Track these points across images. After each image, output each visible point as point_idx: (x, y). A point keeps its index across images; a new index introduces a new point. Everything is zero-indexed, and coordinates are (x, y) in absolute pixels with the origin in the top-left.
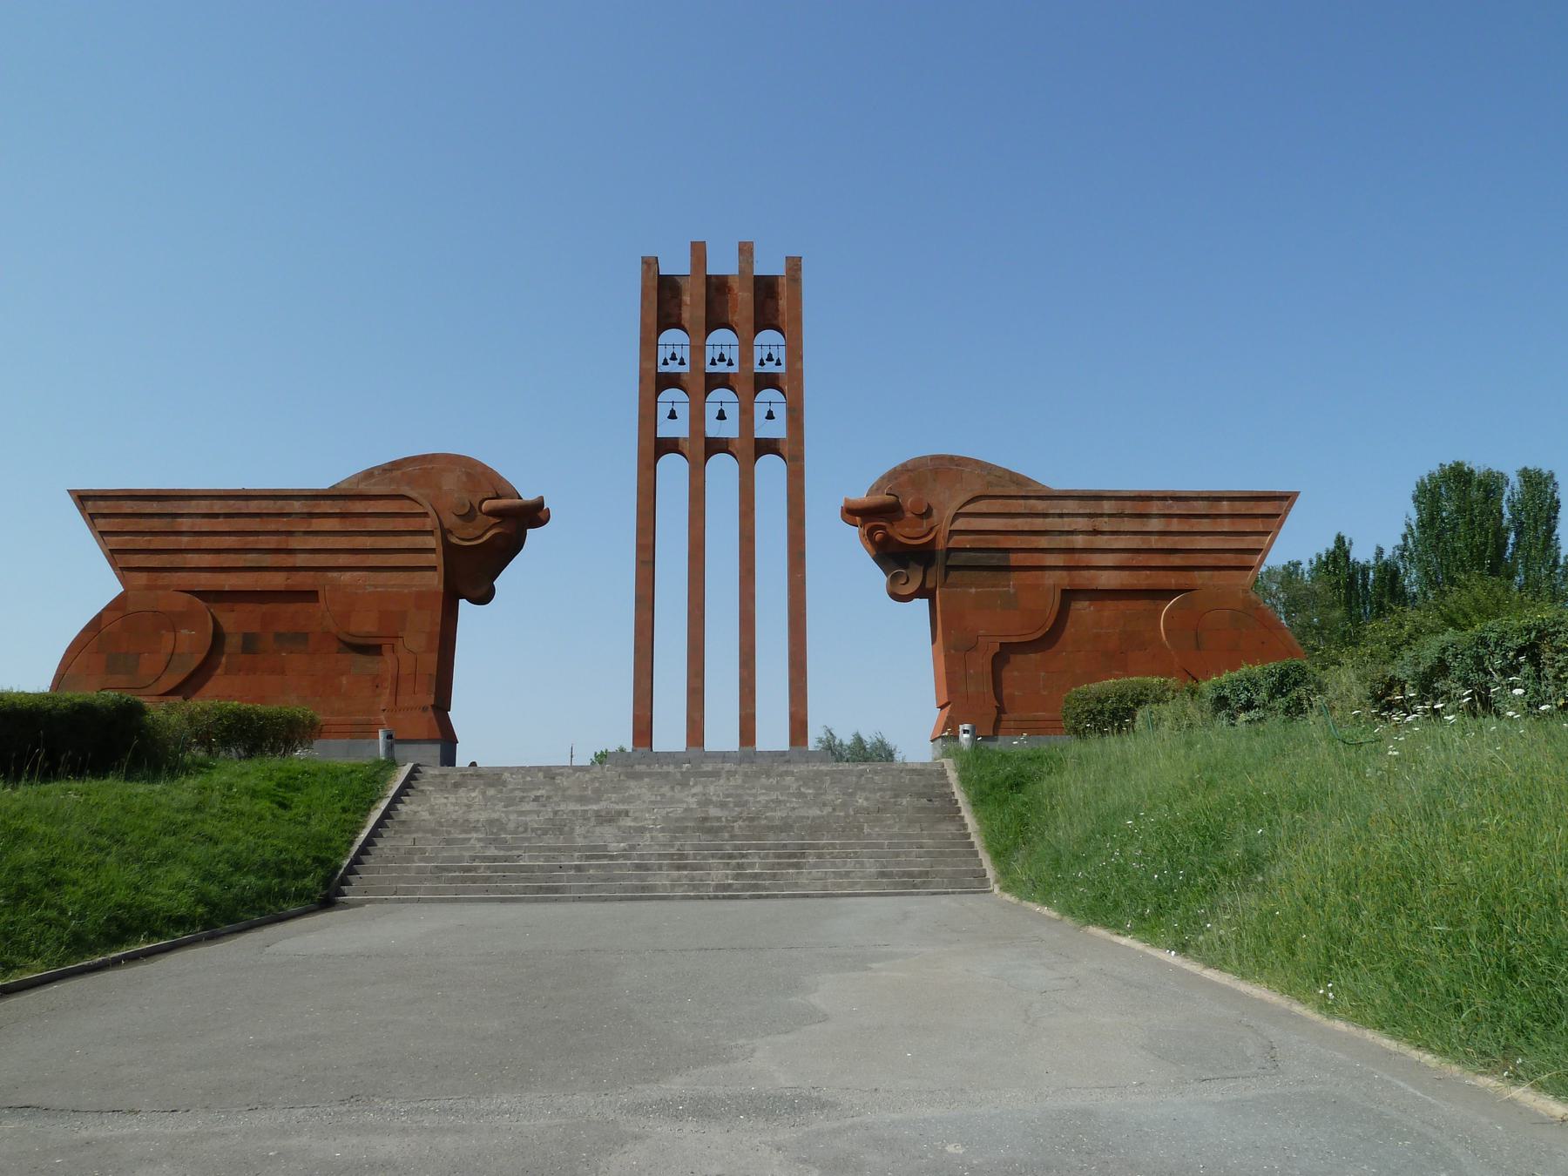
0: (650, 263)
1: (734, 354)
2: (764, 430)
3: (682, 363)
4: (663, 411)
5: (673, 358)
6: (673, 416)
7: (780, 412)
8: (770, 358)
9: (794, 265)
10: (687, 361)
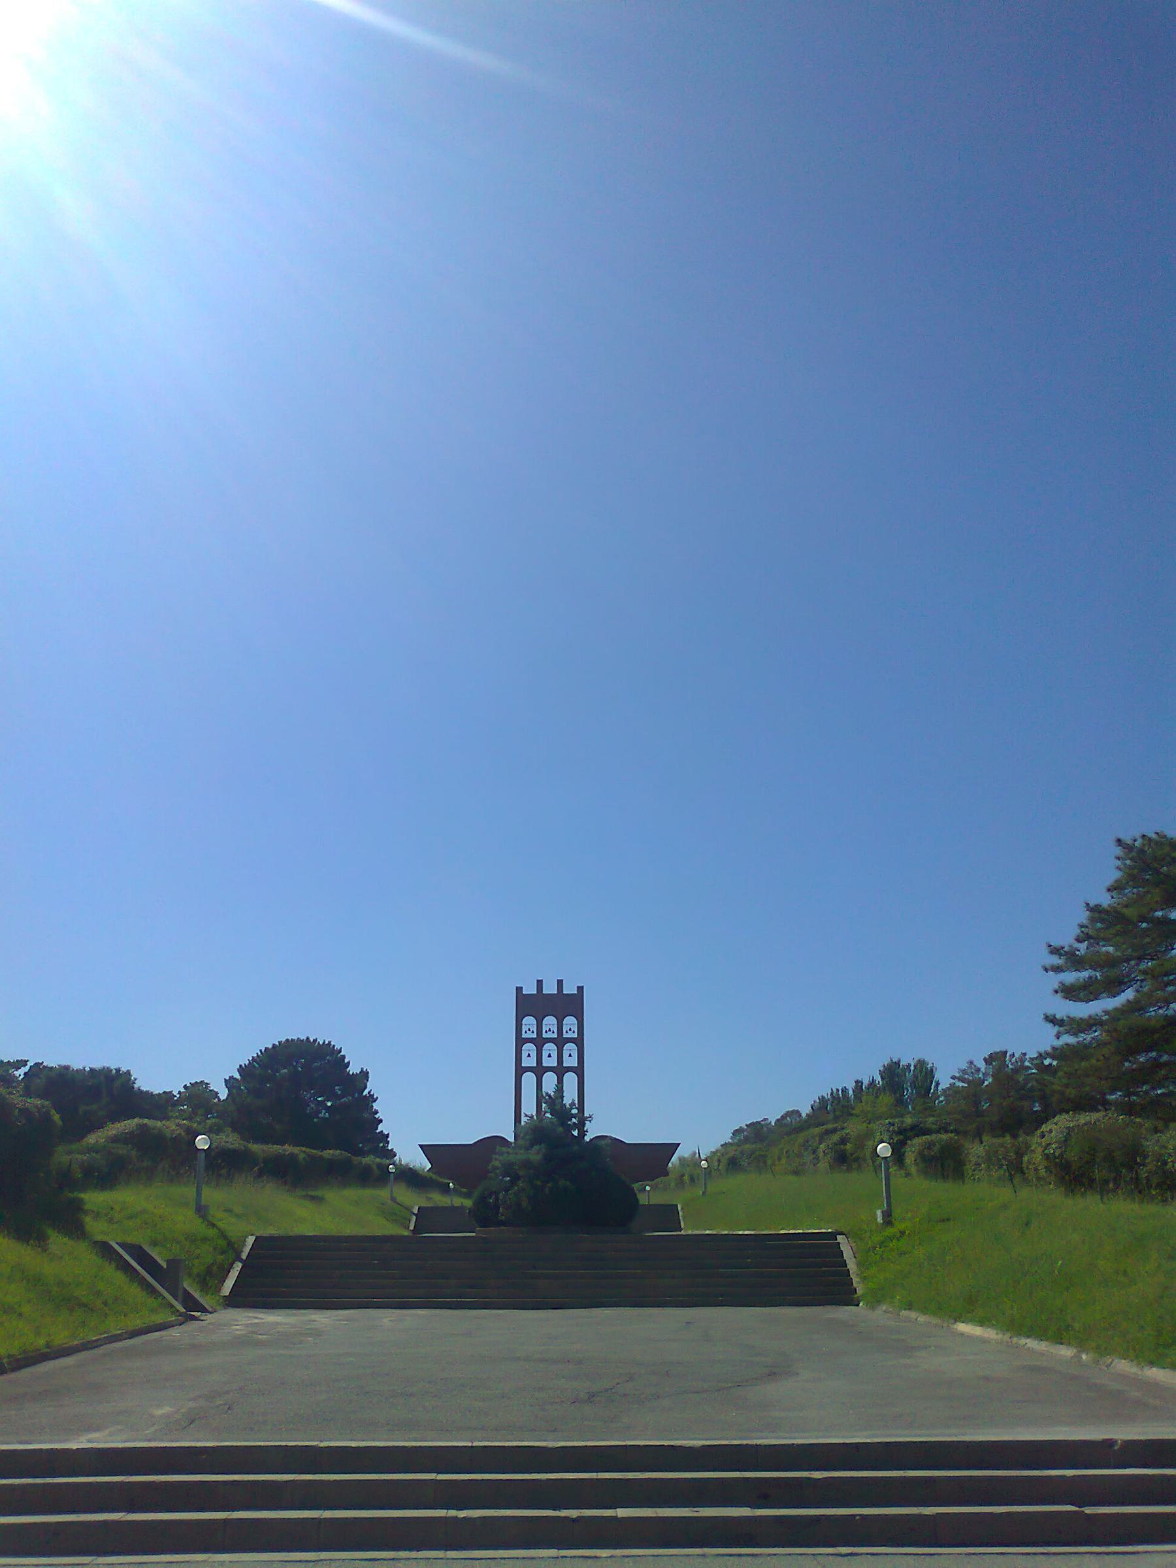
0: (519, 990)
4: (524, 1055)
9: (580, 989)
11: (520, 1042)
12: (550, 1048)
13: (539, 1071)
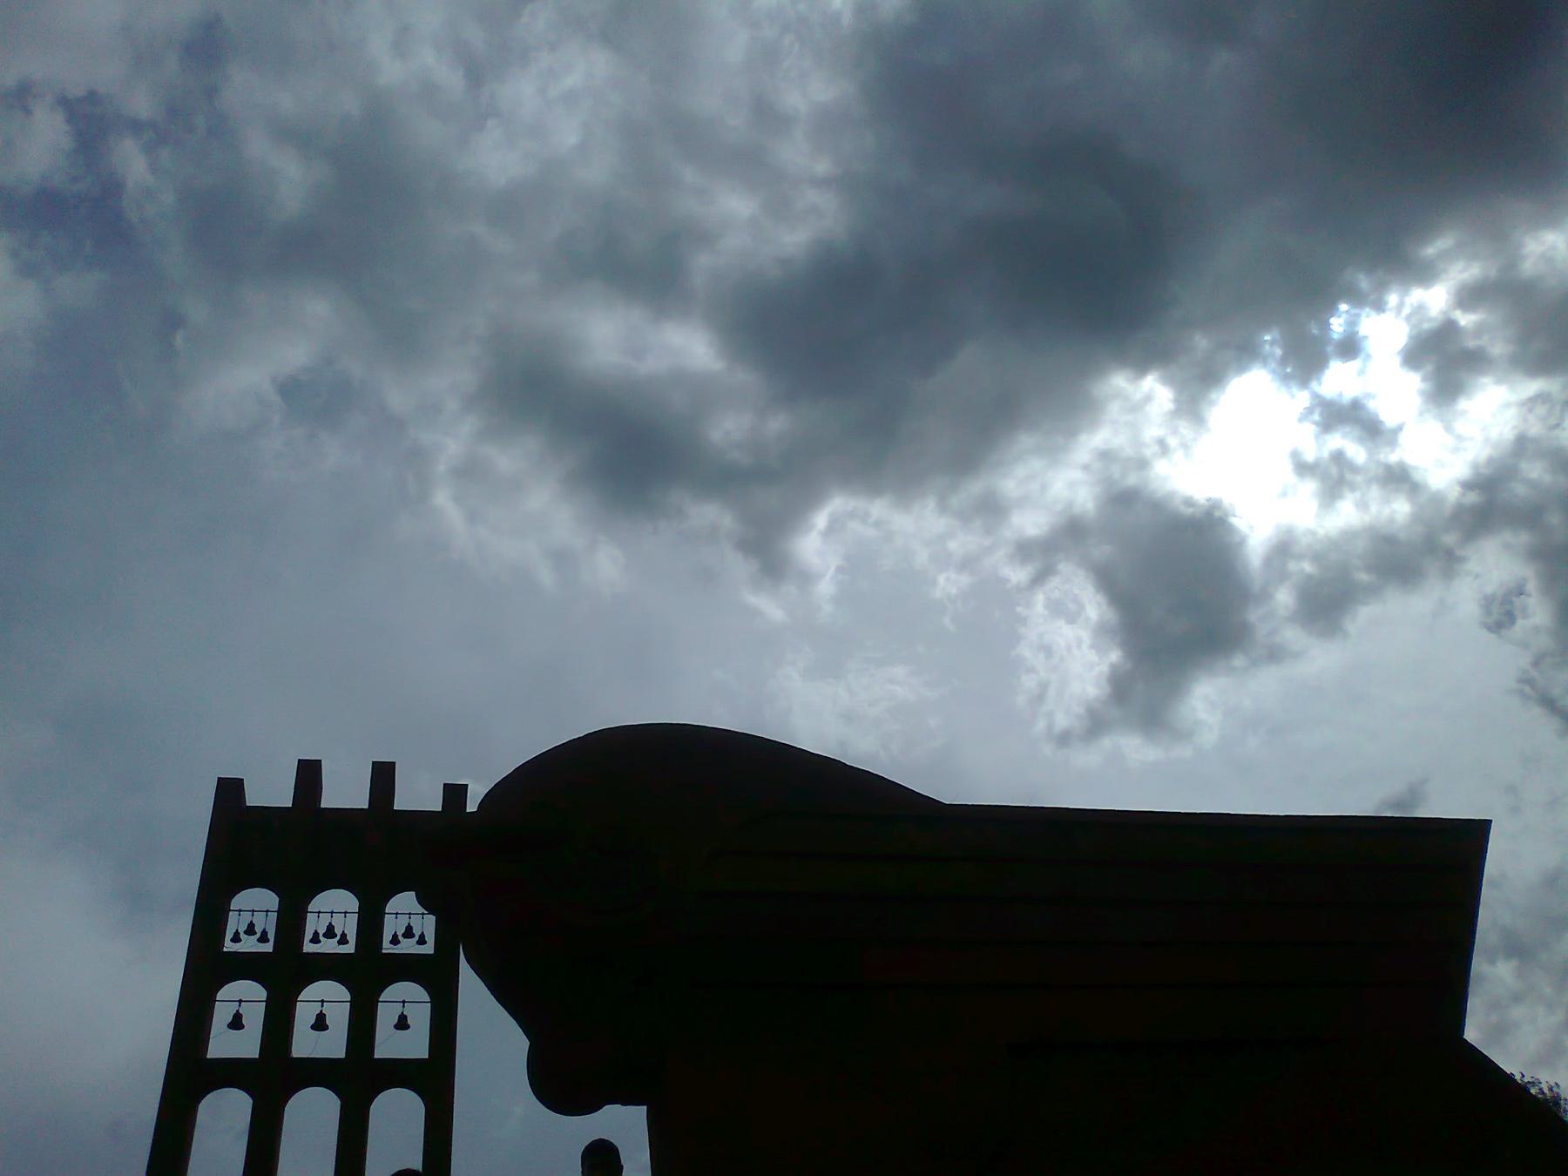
0: (229, 790)
1: (349, 926)
2: (389, 1045)
3: (263, 938)
4: (222, 1015)
5: (250, 930)
6: (236, 1023)
7: (421, 1016)
8: (409, 933)
10: (271, 936)
11: (207, 968)
12: (326, 998)
13: (273, 1078)
